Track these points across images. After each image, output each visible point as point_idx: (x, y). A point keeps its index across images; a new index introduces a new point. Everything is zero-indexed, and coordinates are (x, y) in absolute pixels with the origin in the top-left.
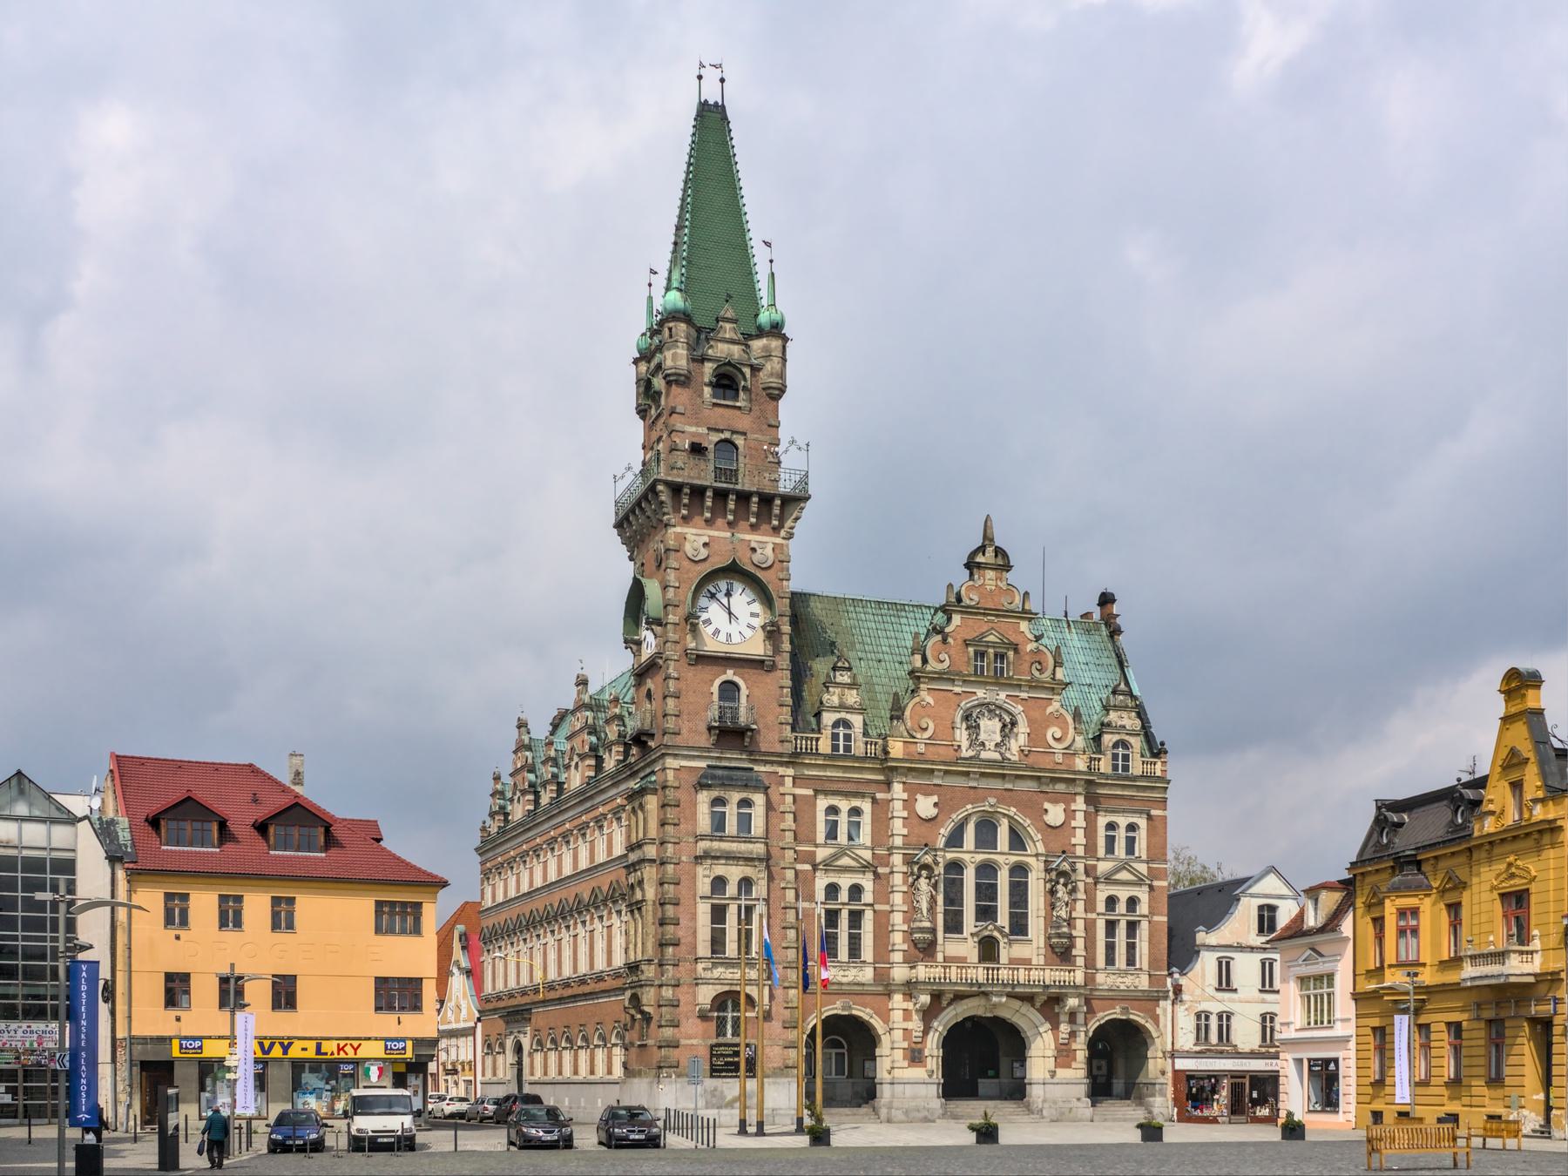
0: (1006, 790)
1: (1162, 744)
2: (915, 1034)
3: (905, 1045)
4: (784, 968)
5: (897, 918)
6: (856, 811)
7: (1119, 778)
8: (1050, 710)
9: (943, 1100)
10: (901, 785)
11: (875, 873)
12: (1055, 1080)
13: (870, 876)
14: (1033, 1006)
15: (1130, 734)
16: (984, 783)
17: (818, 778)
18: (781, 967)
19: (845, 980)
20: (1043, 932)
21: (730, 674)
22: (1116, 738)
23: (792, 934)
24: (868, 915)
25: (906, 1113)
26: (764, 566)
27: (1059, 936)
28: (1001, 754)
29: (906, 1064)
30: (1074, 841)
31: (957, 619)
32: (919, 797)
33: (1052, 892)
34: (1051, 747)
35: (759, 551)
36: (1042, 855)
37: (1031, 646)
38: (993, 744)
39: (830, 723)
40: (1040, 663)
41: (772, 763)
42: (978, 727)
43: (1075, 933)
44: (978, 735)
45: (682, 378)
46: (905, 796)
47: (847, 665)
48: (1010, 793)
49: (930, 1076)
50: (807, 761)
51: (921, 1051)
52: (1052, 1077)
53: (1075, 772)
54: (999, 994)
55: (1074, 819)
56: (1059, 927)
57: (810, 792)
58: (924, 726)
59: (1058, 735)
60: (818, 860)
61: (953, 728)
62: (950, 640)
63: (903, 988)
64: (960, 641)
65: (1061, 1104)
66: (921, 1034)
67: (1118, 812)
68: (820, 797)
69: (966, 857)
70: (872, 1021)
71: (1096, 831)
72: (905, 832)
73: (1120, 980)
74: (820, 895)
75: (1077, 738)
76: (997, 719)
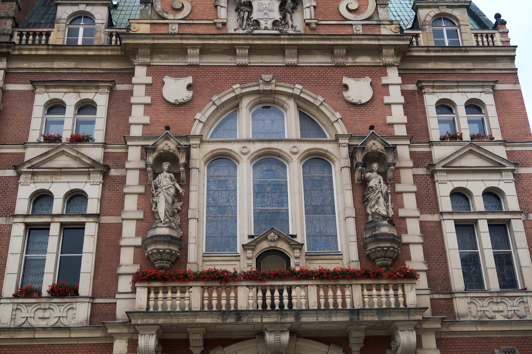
1: (498, 16)
7: (444, 48)
10: (144, 69)
11: (105, 174)
13: (99, 178)
16: (256, 60)
17: (41, 72)
19: (43, 324)
20: (354, 239)
22: (434, 12)
27: (377, 238)
28: (280, 30)
30: (389, 120)
32: (167, 80)
33: (365, 182)
36: (343, 136)
38: (270, 22)
39: (65, 16)
43: (405, 239)
44: (250, 13)
46: (149, 80)
48: (294, 70)
50: (26, 53)
53: (378, 37)
54: (278, 328)
55: (388, 94)
56: (374, 228)
57: (27, 87)
58: (179, 6)
59: (354, 6)
60: (27, 158)
61: (216, 6)
63: (125, 330)
67: (451, 87)
69: (236, 148)
71: (424, 112)
72: (147, 120)
73: (495, 308)
75: (380, 10)
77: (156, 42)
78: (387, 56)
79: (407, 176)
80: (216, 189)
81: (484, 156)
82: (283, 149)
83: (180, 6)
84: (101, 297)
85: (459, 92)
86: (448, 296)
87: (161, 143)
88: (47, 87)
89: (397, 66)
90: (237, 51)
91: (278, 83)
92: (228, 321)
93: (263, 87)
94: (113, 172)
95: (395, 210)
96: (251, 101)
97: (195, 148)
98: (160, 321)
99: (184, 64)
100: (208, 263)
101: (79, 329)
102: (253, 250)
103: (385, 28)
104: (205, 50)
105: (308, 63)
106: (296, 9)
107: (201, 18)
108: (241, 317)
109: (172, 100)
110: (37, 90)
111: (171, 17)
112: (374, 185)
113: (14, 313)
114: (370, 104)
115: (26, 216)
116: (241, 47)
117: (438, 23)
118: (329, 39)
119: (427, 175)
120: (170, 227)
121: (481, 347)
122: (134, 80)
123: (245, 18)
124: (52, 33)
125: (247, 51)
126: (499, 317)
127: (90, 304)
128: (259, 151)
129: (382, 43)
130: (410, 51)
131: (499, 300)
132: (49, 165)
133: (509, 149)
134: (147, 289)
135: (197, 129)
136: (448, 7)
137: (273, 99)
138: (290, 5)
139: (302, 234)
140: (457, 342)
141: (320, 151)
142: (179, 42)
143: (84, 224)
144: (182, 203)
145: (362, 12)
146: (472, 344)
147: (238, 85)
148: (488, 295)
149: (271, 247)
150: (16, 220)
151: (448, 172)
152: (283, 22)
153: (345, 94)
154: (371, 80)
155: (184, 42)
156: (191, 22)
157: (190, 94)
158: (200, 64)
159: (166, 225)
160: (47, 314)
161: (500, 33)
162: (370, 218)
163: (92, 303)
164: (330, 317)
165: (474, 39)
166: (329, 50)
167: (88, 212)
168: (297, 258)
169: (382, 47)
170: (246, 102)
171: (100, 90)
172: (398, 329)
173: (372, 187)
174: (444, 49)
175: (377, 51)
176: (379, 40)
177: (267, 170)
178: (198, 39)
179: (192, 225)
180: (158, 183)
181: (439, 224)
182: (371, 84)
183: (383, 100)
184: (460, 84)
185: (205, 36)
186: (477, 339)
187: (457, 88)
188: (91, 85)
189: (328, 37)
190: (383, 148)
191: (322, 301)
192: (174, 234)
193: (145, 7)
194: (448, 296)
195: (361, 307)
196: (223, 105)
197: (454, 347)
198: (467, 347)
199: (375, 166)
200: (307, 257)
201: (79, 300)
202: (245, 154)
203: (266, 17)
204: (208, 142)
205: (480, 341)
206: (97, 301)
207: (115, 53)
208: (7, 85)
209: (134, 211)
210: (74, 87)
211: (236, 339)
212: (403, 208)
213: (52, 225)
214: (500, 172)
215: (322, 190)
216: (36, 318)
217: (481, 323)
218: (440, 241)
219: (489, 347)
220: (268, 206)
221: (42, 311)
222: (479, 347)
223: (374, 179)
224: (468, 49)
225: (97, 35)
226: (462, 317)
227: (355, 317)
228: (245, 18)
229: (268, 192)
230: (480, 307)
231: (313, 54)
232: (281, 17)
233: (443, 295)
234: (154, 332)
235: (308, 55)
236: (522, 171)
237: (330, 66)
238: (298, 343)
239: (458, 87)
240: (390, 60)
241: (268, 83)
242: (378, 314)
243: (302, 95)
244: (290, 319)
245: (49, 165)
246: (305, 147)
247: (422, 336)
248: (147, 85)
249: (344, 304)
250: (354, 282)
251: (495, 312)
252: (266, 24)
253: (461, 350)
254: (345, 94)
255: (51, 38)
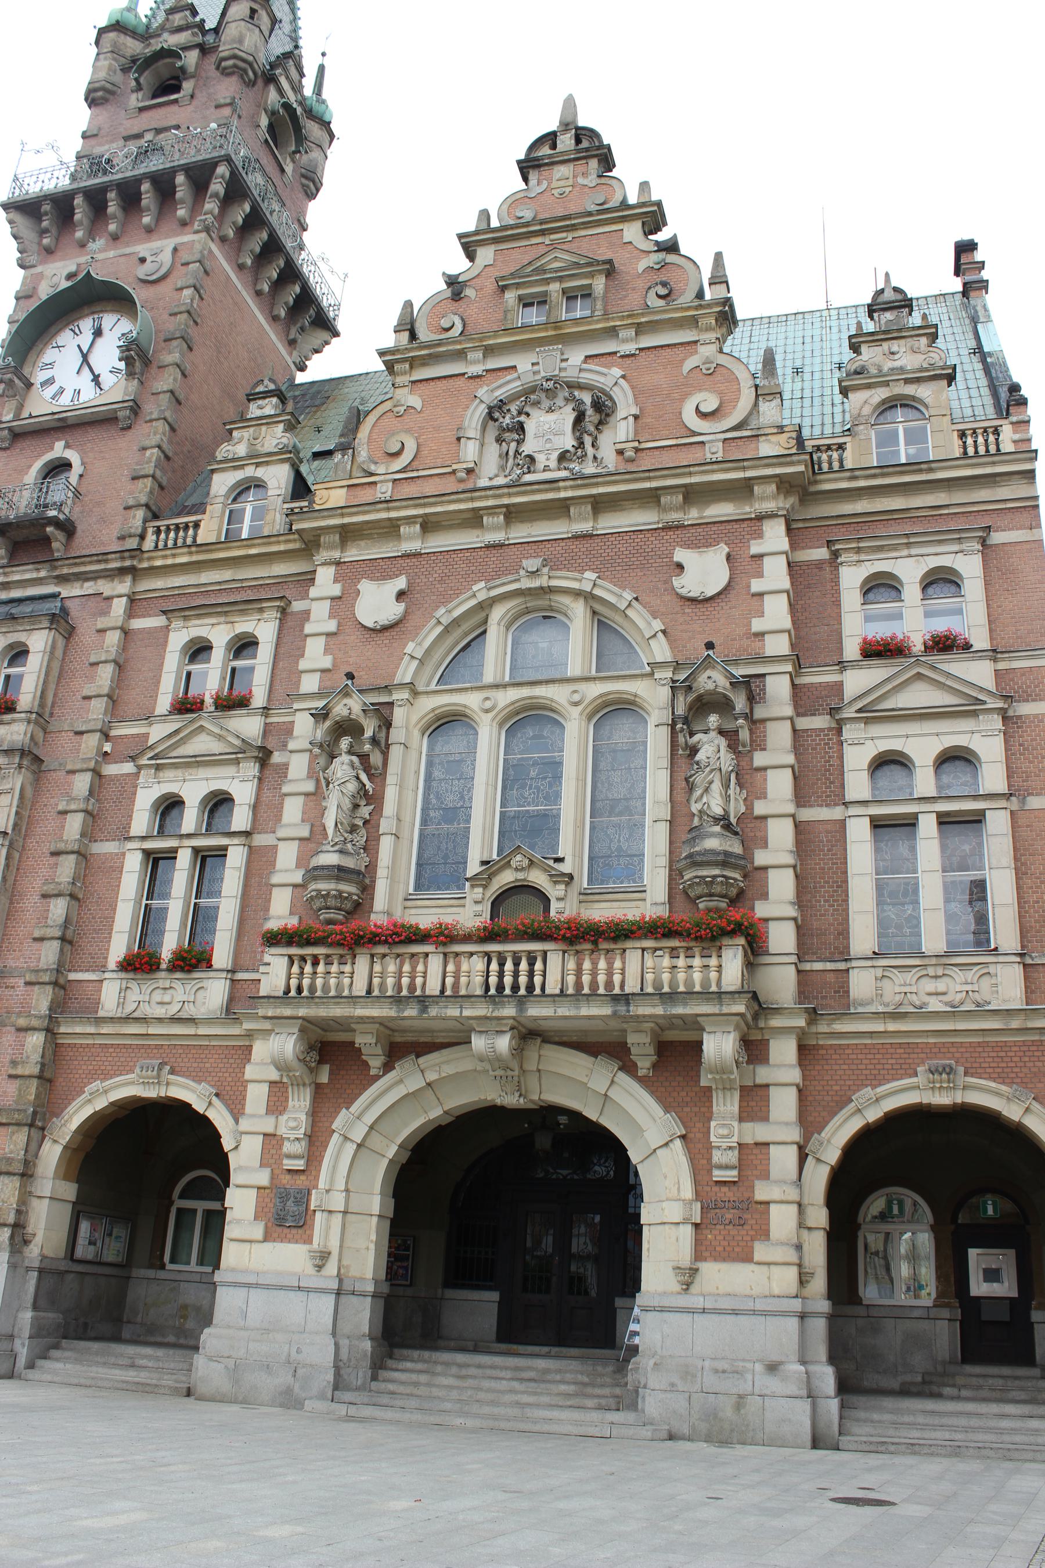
0: (576, 537)
2: (288, 1147)
3: (263, 1178)
4: (28, 983)
5: (287, 856)
6: (244, 645)
8: (690, 363)
9: (367, 1345)
10: (331, 570)
12: (695, 1301)
13: (251, 769)
14: (629, 1067)
15: (918, 380)
16: (521, 533)
17: (181, 592)
18: (21, 982)
19: (160, 1012)
21: (59, 450)
23: (58, 909)
24: (236, 856)
25: (235, 1372)
26: (154, 277)
29: (258, 1231)
30: (757, 625)
31: (486, 255)
34: (695, 434)
35: (149, 259)
37: (642, 266)
38: (555, 455)
39: (223, 490)
40: (664, 284)
41: (94, 576)
42: (521, 428)
43: (761, 858)
44: (520, 442)
45: (100, 94)
47: (272, 387)
48: (587, 544)
49: (320, 1268)
50: (158, 563)
51: (303, 1197)
52: (687, 1286)
54: (490, 1025)
55: (760, 575)
58: (395, 448)
61: (459, 439)
62: (469, 292)
64: (490, 286)
65: (710, 1381)
66: (299, 1148)
67: (894, 548)
68: (176, 624)
69: (472, 701)
70: (211, 1115)
71: (837, 604)
73: (930, 986)
74: (141, 821)
76: (569, 409)
77: (346, 520)
78: (762, 499)
79: (779, 736)
80: (443, 777)
81: (944, 684)
82: (555, 698)
83: (399, 445)
84: (247, 970)
85: (911, 556)
86: (842, 966)
87: (337, 703)
88: (186, 618)
89: (784, 516)
90: (485, 519)
91: (553, 573)
92: (406, 1014)
93: (526, 583)
94: (277, 758)
95: (748, 803)
96: (508, 611)
97: (400, 706)
98: (302, 1012)
99: (396, 554)
100: (413, 911)
101: (209, 1021)
102: (485, 887)
103: (769, 441)
104: (429, 525)
105: (614, 527)
106: (607, 423)
107: (432, 465)
108: (426, 1007)
109: (370, 625)
110: (173, 626)
111: (381, 470)
112: (704, 758)
113: (122, 994)
114: (722, 596)
115: (143, 838)
116: (490, 511)
117: (889, 415)
118: (649, 479)
119: (830, 729)
120: (341, 852)
121: (894, 1061)
122: (313, 592)
123: (511, 453)
124: (202, 524)
125: (502, 517)
126: (935, 1005)
127: (228, 981)
128: (513, 703)
129: (750, 474)
130: (816, 482)
131: (940, 972)
132: (181, 751)
133: (1001, 666)
134: (286, 958)
135: (406, 672)
136: (907, 381)
137: (547, 603)
138: (591, 419)
139: (578, 855)
140: (847, 1052)
141: (625, 696)
142: (384, 515)
143: (225, 848)
144: (372, 807)
145: (725, 416)
146: (877, 1056)
147: (482, 584)
148: (917, 962)
149: (517, 880)
150: (131, 845)
151: (867, 721)
152: (579, 453)
153: (676, 582)
154: (727, 550)
155: (393, 514)
156: (415, 474)
157: (399, 609)
158: (423, 551)
159: (336, 848)
160: (167, 998)
161: (1012, 423)
162: (696, 822)
163: (232, 981)
164: (578, 1008)
165: (957, 442)
166: (651, 498)
167: (234, 828)
168: (559, 899)
169: (752, 482)
170: (497, 613)
171: (265, 615)
172: (703, 1030)
173: (698, 763)
174: (886, 470)
175: (743, 489)
176: (744, 469)
177: (534, 737)
178: (416, 506)
179: (386, 845)
180: (331, 774)
181: (842, 824)
182: (729, 557)
183: (749, 586)
184: (912, 540)
185: (426, 500)
186: (889, 1046)
187: (908, 548)
188: (250, 607)
189: (647, 474)
190: (728, 685)
191: (571, 979)
192: (349, 863)
193: (343, 456)
194: (842, 966)
195: (637, 990)
196: (456, 622)
197: (841, 1062)
198: (867, 1062)
199: (713, 720)
200: (581, 897)
201: (212, 974)
202: (487, 711)
203: (548, 446)
204: (427, 693)
205: (892, 1051)
206: (240, 976)
207: (291, 546)
208: (132, 621)
209: (295, 825)
210: (226, 613)
211: (442, 1043)
212: (765, 798)
213: (180, 850)
214: (974, 714)
215: (630, 769)
216: (153, 1003)
217: (896, 1016)
218: (840, 859)
219: (910, 1061)
220: (529, 805)
221: (162, 992)
222: (890, 1061)
223: (706, 746)
224: (933, 465)
225: (269, 518)
226: (861, 1005)
227: (622, 1009)
228: (511, 453)
229: (532, 779)
230: (901, 985)
231: (624, 510)
232: (575, 444)
233: (833, 964)
234: (296, 1030)
235: (615, 511)
236: (1025, 709)
237: (655, 529)
238: (542, 1052)
239: (908, 545)
240: (769, 506)
241: (534, 574)
242: (663, 1003)
243: (597, 592)
244: (509, 1011)
245: (180, 752)
246: (595, 690)
247: (772, 1042)
248: (333, 599)
249: (609, 984)
250: (629, 944)
251: (929, 994)
252: (548, 459)
253: (855, 1067)
254: (676, 582)
255: (200, 532)
